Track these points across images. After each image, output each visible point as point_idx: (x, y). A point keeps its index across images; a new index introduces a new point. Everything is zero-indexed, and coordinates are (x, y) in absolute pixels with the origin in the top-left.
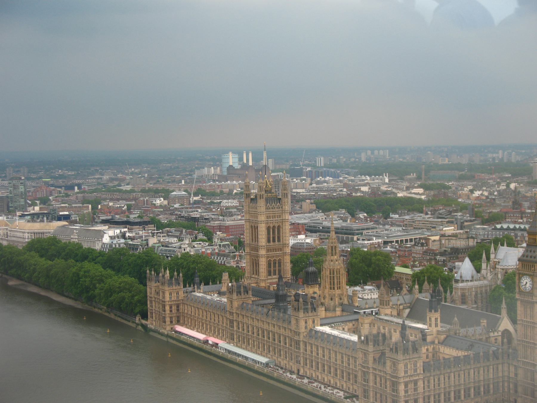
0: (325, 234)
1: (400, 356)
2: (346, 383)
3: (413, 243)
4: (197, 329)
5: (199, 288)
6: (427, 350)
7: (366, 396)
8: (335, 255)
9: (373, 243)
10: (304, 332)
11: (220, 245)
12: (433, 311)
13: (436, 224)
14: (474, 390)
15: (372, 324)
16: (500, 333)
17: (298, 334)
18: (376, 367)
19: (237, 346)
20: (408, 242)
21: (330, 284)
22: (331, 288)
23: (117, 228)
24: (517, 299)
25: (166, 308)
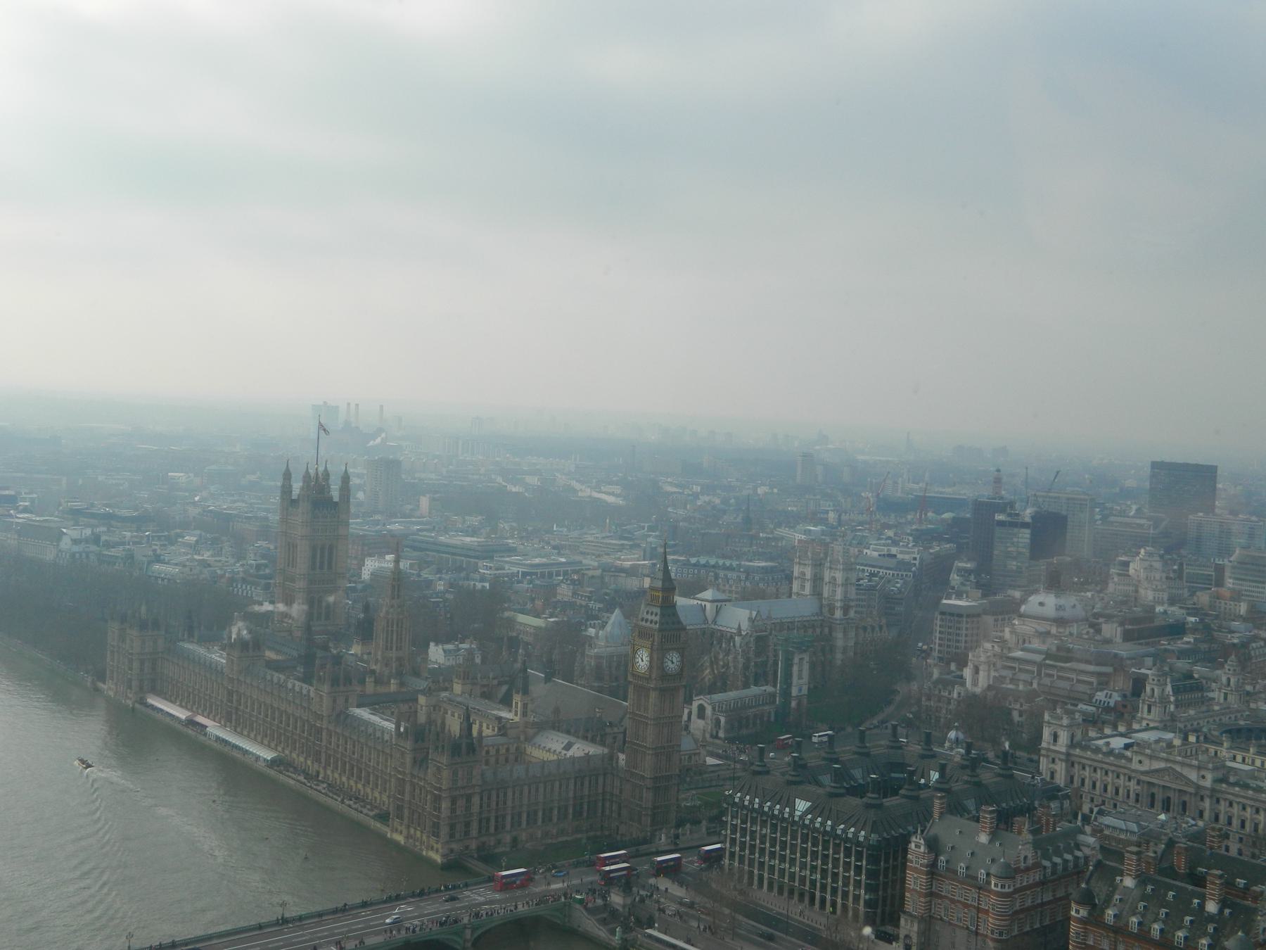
0: (434, 553)
1: (444, 760)
2: (381, 796)
3: (562, 578)
4: (181, 701)
5: (191, 635)
6: (508, 750)
7: (400, 817)
8: (398, 598)
9: (504, 574)
10: (329, 716)
11: (251, 566)
12: (521, 692)
13: (613, 549)
14: (559, 812)
15: (437, 708)
16: (622, 730)
17: (320, 717)
18: (416, 774)
19: (235, 731)
20: (560, 575)
21: (387, 642)
22: (387, 649)
23: (87, 526)
24: (630, 682)
25: (134, 664)
